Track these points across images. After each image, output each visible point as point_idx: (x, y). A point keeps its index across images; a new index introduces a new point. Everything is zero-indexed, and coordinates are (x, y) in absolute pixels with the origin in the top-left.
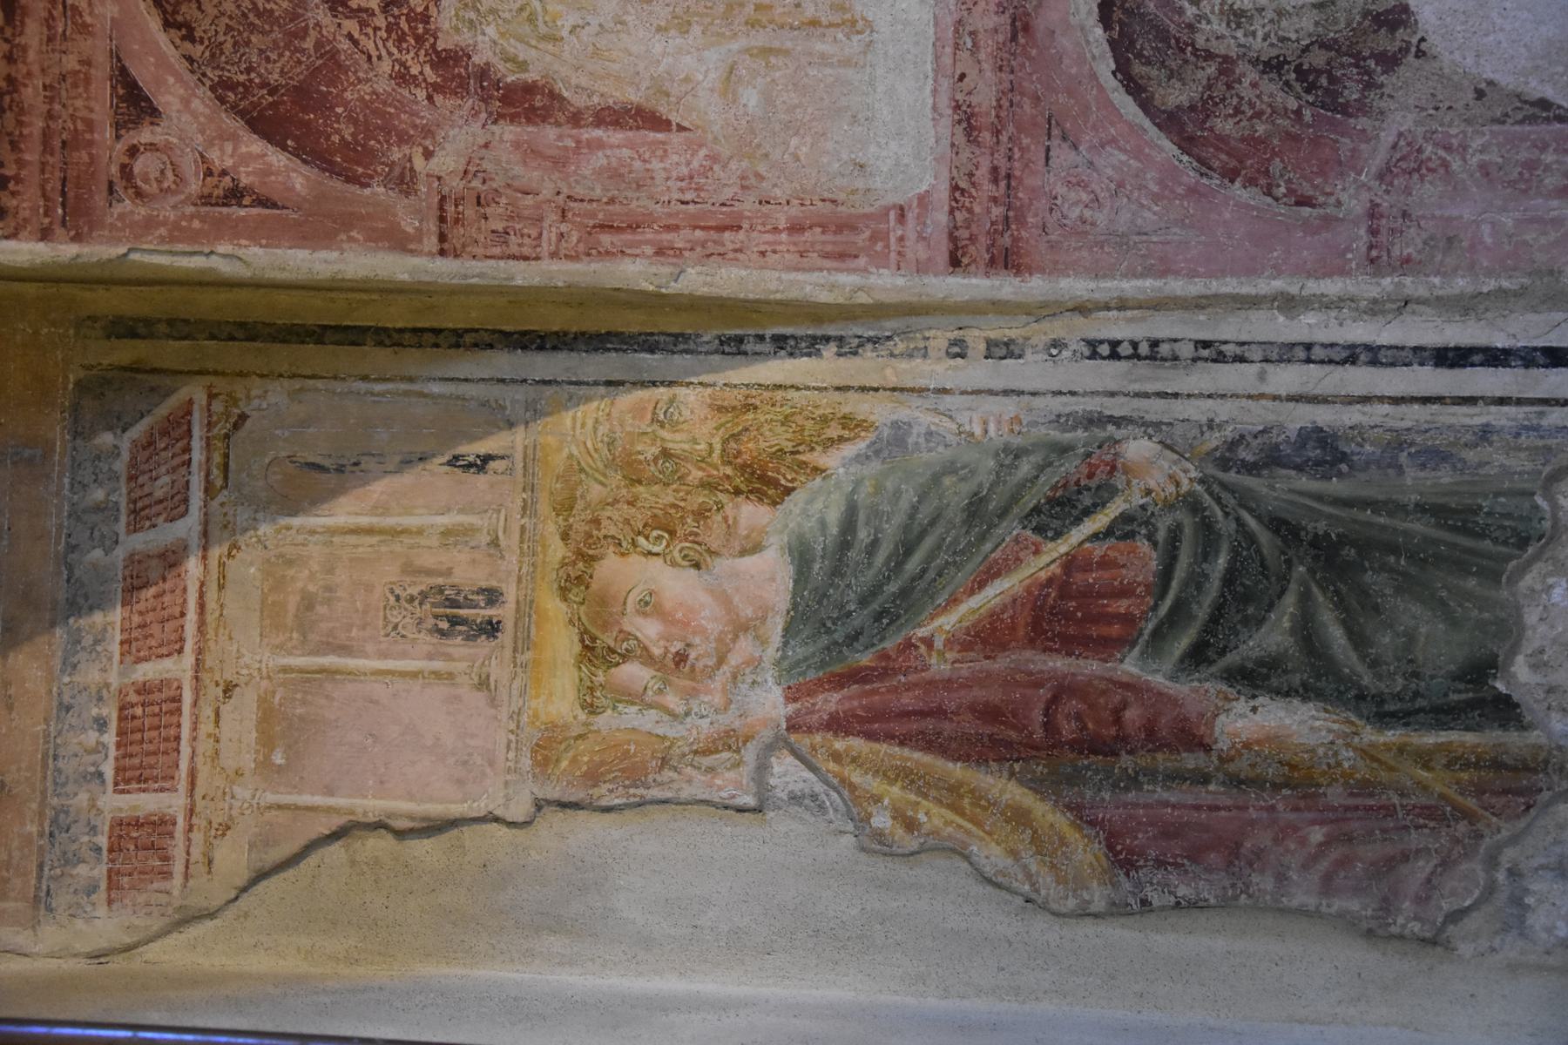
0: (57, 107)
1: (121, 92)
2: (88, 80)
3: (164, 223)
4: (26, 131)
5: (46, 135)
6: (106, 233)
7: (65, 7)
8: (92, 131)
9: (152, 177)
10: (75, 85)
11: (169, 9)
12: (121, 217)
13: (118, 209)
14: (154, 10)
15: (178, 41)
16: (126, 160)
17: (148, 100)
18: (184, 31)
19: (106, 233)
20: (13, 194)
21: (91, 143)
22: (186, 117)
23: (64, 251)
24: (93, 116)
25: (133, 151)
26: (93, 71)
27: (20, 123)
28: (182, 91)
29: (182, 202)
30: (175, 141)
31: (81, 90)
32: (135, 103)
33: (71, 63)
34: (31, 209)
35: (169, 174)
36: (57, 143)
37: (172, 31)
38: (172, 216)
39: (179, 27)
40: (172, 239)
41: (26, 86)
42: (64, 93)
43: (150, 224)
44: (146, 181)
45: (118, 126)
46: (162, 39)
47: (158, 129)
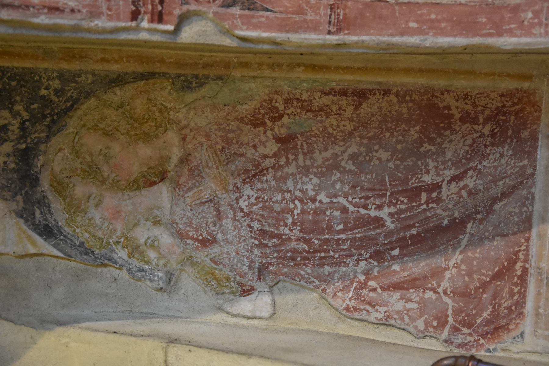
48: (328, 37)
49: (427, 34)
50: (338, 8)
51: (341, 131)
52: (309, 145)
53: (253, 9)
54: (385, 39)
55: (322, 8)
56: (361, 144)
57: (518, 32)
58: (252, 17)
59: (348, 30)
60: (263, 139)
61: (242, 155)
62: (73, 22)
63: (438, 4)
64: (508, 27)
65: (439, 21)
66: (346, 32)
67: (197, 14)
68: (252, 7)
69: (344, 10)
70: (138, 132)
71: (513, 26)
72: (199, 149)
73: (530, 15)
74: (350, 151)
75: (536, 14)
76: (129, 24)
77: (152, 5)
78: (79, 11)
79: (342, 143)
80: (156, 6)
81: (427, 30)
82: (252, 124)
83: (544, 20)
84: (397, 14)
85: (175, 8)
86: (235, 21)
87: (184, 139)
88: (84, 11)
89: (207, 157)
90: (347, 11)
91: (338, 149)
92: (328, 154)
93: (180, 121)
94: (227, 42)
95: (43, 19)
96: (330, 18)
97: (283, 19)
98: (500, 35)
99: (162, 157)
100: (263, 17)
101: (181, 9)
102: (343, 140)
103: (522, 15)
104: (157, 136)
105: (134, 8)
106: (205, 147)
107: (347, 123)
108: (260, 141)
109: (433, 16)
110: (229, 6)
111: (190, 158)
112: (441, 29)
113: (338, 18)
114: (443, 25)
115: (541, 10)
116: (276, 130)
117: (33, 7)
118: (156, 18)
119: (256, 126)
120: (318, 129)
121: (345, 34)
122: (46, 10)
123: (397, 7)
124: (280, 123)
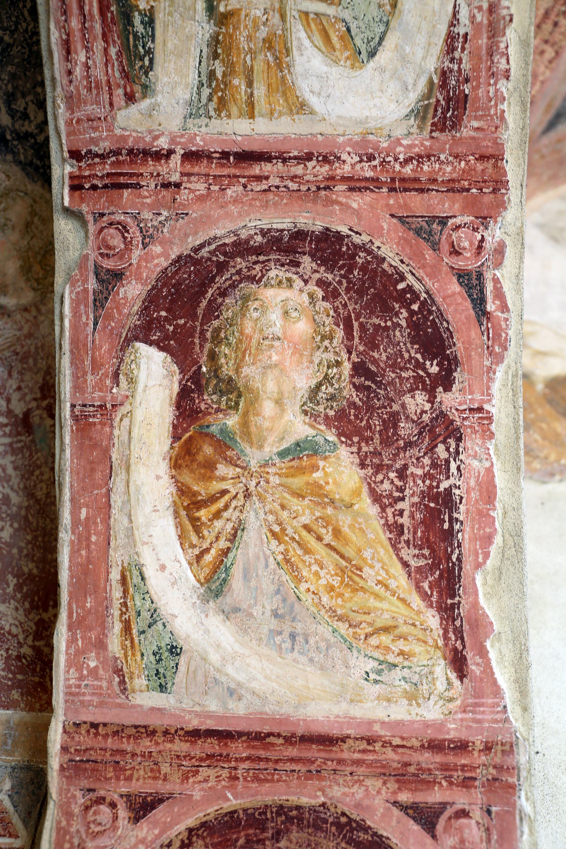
0: (139, 759)
1: (149, 799)
2: (155, 778)
3: (69, 825)
4: (124, 740)
5: (123, 752)
6: (65, 787)
7: (197, 766)
8: (126, 779)
9: (97, 817)
10: (152, 770)
11: (200, 832)
12: (74, 796)
13: (79, 794)
14: (198, 822)
15: (180, 837)
16: (108, 800)
17: (144, 816)
18: (187, 841)
19: (65, 787)
20: (88, 731)
21: (118, 779)
22: (133, 840)
23: (55, 762)
24: (134, 781)
25: (113, 805)
26: (160, 782)
27: (129, 737)
28: (149, 839)
29: (81, 838)
30: (119, 833)
31: (149, 774)
32: (142, 807)
33: (165, 768)
34: (79, 741)
35: (98, 829)
36: (118, 758)
37: (186, 834)
38: (73, 829)
39: (189, 838)
40: (59, 829)
41: (151, 741)
42: (147, 764)
43: (69, 815)
44: (95, 813)
45: (128, 796)
46: (181, 827)
47: (126, 822)
48: (68, 405)
49: (73, 533)
50: (102, 415)
51: (35, 486)
52: (21, 450)
53: (95, 305)
54: (68, 479)
55: (101, 394)
56: (20, 508)
57: (72, 651)
58: (86, 306)
59: (77, 429)
60: (28, 398)
61: (10, 375)
62: (57, 75)
63: (109, 544)
64: (79, 636)
65: (88, 547)
66: (74, 428)
67: (87, 237)
68: (97, 304)
69: (100, 423)
70: (31, 259)
71: (80, 643)
72: (15, 327)
73: (92, 664)
74: (13, 496)
75: (94, 672)
76: (65, 149)
77: (89, 176)
78: (71, 82)
79: (22, 486)
80: (90, 181)
81: (77, 531)
82: (43, 385)
83: (85, 682)
84: (96, 492)
85: (88, 206)
86: (80, 283)
87: (26, 310)
88: (72, 88)
89: (6, 336)
90: (99, 427)
91: (15, 481)
92: (10, 470)
93: (44, 304)
94: (59, 279)
95: (55, 36)
96: (90, 406)
97: (85, 345)
98: (70, 628)
99: (6, 286)
100: (87, 319)
101: (88, 213)
102: (25, 488)
103: (93, 654)
104: (28, 280)
105: (83, 153)
106: (18, 333)
107: (44, 491)
108: (25, 394)
109: (94, 538)
110: (97, 275)
111: (6, 317)
112: (79, 550)
113: (90, 416)
114: (83, 552)
115: (97, 678)
116: (38, 412)
117: (66, 21)
118: (76, 182)
119: (42, 389)
120: (38, 459)
121: (72, 426)
122: (64, 37)
123: (104, 490)
124: (45, 415)
